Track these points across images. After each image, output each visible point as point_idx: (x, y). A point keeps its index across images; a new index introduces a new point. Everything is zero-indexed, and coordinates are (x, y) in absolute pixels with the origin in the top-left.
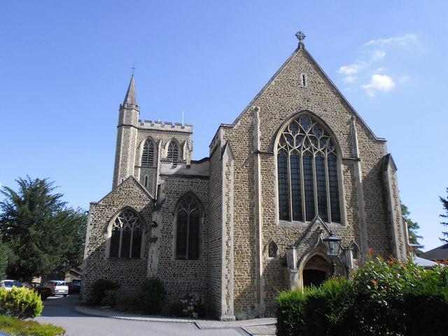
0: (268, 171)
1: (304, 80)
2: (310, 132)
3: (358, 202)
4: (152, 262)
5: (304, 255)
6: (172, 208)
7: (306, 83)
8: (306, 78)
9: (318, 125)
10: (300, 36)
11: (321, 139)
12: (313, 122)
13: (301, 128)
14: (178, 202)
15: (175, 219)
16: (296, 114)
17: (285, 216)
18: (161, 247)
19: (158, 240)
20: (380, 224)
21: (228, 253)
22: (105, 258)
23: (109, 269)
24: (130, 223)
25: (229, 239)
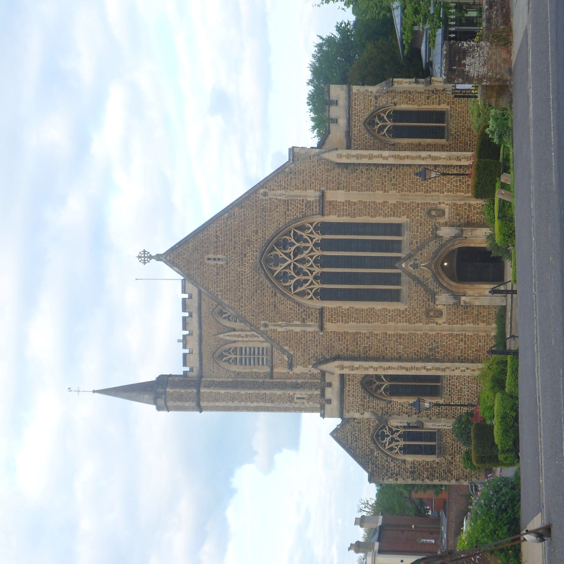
0: (346, 317)
1: (215, 259)
2: (288, 255)
3: (378, 201)
4: (444, 426)
5: (441, 285)
6: (382, 404)
7: (220, 256)
8: (211, 256)
9: (277, 245)
10: (145, 257)
11: (298, 241)
12: (272, 249)
13: (285, 268)
14: (374, 397)
15: (395, 399)
16: (265, 273)
17: (395, 296)
18: (428, 417)
19: (419, 419)
20: (405, 174)
21: (437, 369)
22: (437, 460)
23: (450, 455)
24: (393, 433)
25: (425, 368)
